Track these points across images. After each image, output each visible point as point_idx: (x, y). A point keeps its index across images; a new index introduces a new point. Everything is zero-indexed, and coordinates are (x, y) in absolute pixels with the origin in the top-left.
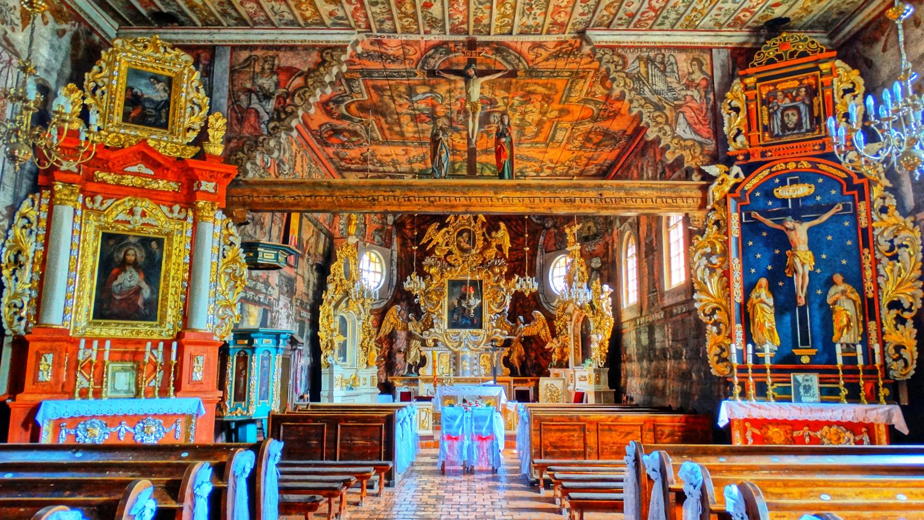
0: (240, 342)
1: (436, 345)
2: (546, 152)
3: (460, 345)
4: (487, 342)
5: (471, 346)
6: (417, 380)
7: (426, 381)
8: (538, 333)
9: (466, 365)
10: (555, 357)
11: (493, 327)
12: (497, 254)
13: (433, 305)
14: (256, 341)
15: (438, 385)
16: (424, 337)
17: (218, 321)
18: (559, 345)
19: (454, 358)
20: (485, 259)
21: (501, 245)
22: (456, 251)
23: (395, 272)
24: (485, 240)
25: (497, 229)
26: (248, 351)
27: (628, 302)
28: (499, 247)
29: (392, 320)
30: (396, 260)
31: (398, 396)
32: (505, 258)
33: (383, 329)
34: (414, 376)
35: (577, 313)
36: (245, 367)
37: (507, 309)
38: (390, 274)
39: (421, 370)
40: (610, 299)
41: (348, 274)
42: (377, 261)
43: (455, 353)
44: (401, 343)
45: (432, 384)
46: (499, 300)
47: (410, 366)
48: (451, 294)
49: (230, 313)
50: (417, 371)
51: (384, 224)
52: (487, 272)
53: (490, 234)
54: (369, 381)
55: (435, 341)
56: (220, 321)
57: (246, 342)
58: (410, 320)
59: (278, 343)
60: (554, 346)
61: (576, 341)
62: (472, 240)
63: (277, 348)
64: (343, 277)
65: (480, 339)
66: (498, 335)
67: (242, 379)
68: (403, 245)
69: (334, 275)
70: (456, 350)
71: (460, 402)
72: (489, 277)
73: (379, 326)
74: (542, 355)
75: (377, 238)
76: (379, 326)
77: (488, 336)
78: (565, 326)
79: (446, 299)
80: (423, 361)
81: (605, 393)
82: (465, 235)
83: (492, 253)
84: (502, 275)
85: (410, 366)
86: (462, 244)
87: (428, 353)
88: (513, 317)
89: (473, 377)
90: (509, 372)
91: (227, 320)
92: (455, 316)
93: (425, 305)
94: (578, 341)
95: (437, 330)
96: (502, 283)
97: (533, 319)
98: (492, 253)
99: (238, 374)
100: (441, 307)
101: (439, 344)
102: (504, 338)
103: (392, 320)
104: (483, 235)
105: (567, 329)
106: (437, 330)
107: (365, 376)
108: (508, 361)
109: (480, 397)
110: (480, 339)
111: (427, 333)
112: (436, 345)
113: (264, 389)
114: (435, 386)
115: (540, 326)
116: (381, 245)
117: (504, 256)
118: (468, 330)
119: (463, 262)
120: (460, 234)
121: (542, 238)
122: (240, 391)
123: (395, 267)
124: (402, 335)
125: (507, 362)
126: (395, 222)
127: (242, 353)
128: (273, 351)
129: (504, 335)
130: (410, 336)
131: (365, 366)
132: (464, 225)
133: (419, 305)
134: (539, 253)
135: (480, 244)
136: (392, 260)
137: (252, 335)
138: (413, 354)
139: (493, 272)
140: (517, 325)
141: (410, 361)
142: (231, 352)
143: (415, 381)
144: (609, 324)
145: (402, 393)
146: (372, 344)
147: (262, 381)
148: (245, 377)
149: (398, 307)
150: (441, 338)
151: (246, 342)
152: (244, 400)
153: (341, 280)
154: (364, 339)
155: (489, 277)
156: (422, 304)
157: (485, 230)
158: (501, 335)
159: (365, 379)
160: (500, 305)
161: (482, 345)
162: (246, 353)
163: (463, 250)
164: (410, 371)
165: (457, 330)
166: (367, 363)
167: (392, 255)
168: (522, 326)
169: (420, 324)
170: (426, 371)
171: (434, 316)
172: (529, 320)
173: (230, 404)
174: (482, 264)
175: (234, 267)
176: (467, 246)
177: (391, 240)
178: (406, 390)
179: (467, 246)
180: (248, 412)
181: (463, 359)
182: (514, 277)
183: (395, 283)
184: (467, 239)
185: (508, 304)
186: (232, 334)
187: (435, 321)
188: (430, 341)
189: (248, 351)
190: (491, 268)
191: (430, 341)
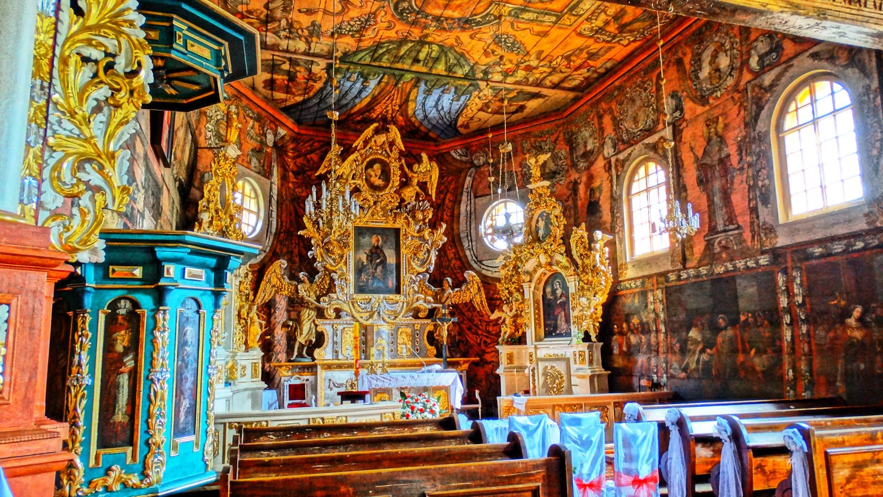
0: (120, 271)
1: (338, 317)
2: (545, 34)
3: (371, 316)
4: (407, 312)
5: (386, 318)
6: (316, 366)
7: (329, 367)
8: (471, 301)
9: (382, 342)
10: (506, 330)
11: (416, 292)
12: (418, 195)
13: (334, 260)
14: (172, 270)
15: (363, 372)
16: (322, 304)
17: (53, 200)
18: (511, 314)
19: (365, 335)
20: (403, 200)
21: (426, 183)
22: (365, 188)
23: (274, 214)
24: (404, 175)
25: (419, 161)
26: (146, 301)
27: (632, 254)
28: (423, 186)
29: (274, 281)
30: (275, 197)
31: (287, 391)
32: (430, 201)
33: (260, 294)
34: (307, 361)
35: (541, 271)
36: (134, 346)
37: (432, 268)
38: (269, 215)
39: (317, 352)
40: (607, 249)
41: (225, 203)
42: (253, 195)
43: (365, 328)
44: (281, 315)
45: (353, 371)
46: (421, 255)
47: (301, 346)
48: (358, 246)
49: (96, 179)
50: (310, 353)
51: (263, 143)
52: (406, 218)
53: (410, 167)
54: (248, 371)
55: (338, 311)
56: (60, 201)
57: (138, 272)
58: (300, 281)
59: (220, 280)
60: (503, 315)
61: (537, 308)
62: (386, 174)
63: (217, 295)
64: (219, 206)
65: (398, 307)
66: (421, 302)
67: (124, 380)
68: (284, 178)
69: (209, 202)
70: (365, 323)
71: (396, 395)
72: (408, 224)
73: (256, 289)
74: (469, 329)
75: (254, 162)
76: (256, 289)
77: (408, 303)
78: (520, 290)
79: (352, 253)
80: (320, 339)
81: (598, 376)
82: (377, 166)
83: (409, 193)
84: (425, 224)
85: (301, 346)
86: (373, 179)
87: (325, 327)
88: (436, 280)
89: (390, 360)
90: (435, 352)
91: (85, 201)
92: (364, 277)
93: (323, 260)
94: (538, 309)
95: (340, 295)
96: (426, 233)
97: (465, 281)
98: (409, 193)
99: (112, 364)
100: (346, 263)
101: (343, 314)
102: (429, 307)
103: (274, 281)
104: (401, 168)
105: (523, 294)
106: (340, 295)
107: (244, 363)
108: (434, 338)
109: (426, 389)
110: (398, 307)
111: (326, 299)
112: (338, 317)
113: (186, 403)
114: (357, 374)
115: (474, 290)
116: (259, 173)
117: (428, 196)
118: (382, 296)
119: (375, 203)
120: (370, 165)
121: (469, 180)
122: (120, 417)
123: (274, 208)
124: (282, 304)
125: (432, 339)
126: (275, 143)
127: (124, 308)
128: (207, 301)
129: (429, 302)
130: (296, 304)
131: (243, 347)
132: (376, 154)
133: (314, 259)
134: (464, 198)
135: (396, 180)
136: (271, 197)
137: (162, 253)
138: (306, 329)
139: (414, 217)
140: (443, 291)
141: (301, 339)
142: (88, 301)
143: (312, 369)
144: (605, 283)
145: (290, 386)
146: (254, 314)
147: (180, 379)
148: (134, 375)
149: (283, 263)
150: (345, 307)
151: (138, 272)
152: (131, 442)
153: (217, 211)
154: (241, 307)
155: (408, 224)
156: (319, 259)
157: (403, 161)
158: (424, 304)
159: (244, 368)
160: (423, 263)
161: (400, 317)
162: (136, 305)
163: (373, 187)
164: (300, 355)
165: (366, 296)
166: (246, 343)
167: (271, 190)
168: (450, 291)
169: (315, 286)
170: (323, 354)
171: (335, 276)
172: (459, 283)
173: (85, 457)
174: (399, 207)
175: (111, 44)
176: (379, 182)
177: (270, 167)
178: (298, 382)
179: (379, 182)
180: (144, 475)
181: (379, 334)
182: (441, 226)
183: (274, 231)
184: (379, 173)
185: (433, 262)
186: (101, 244)
187: (336, 283)
188: (331, 313)
189: (146, 301)
190: (412, 212)
191: (331, 313)
